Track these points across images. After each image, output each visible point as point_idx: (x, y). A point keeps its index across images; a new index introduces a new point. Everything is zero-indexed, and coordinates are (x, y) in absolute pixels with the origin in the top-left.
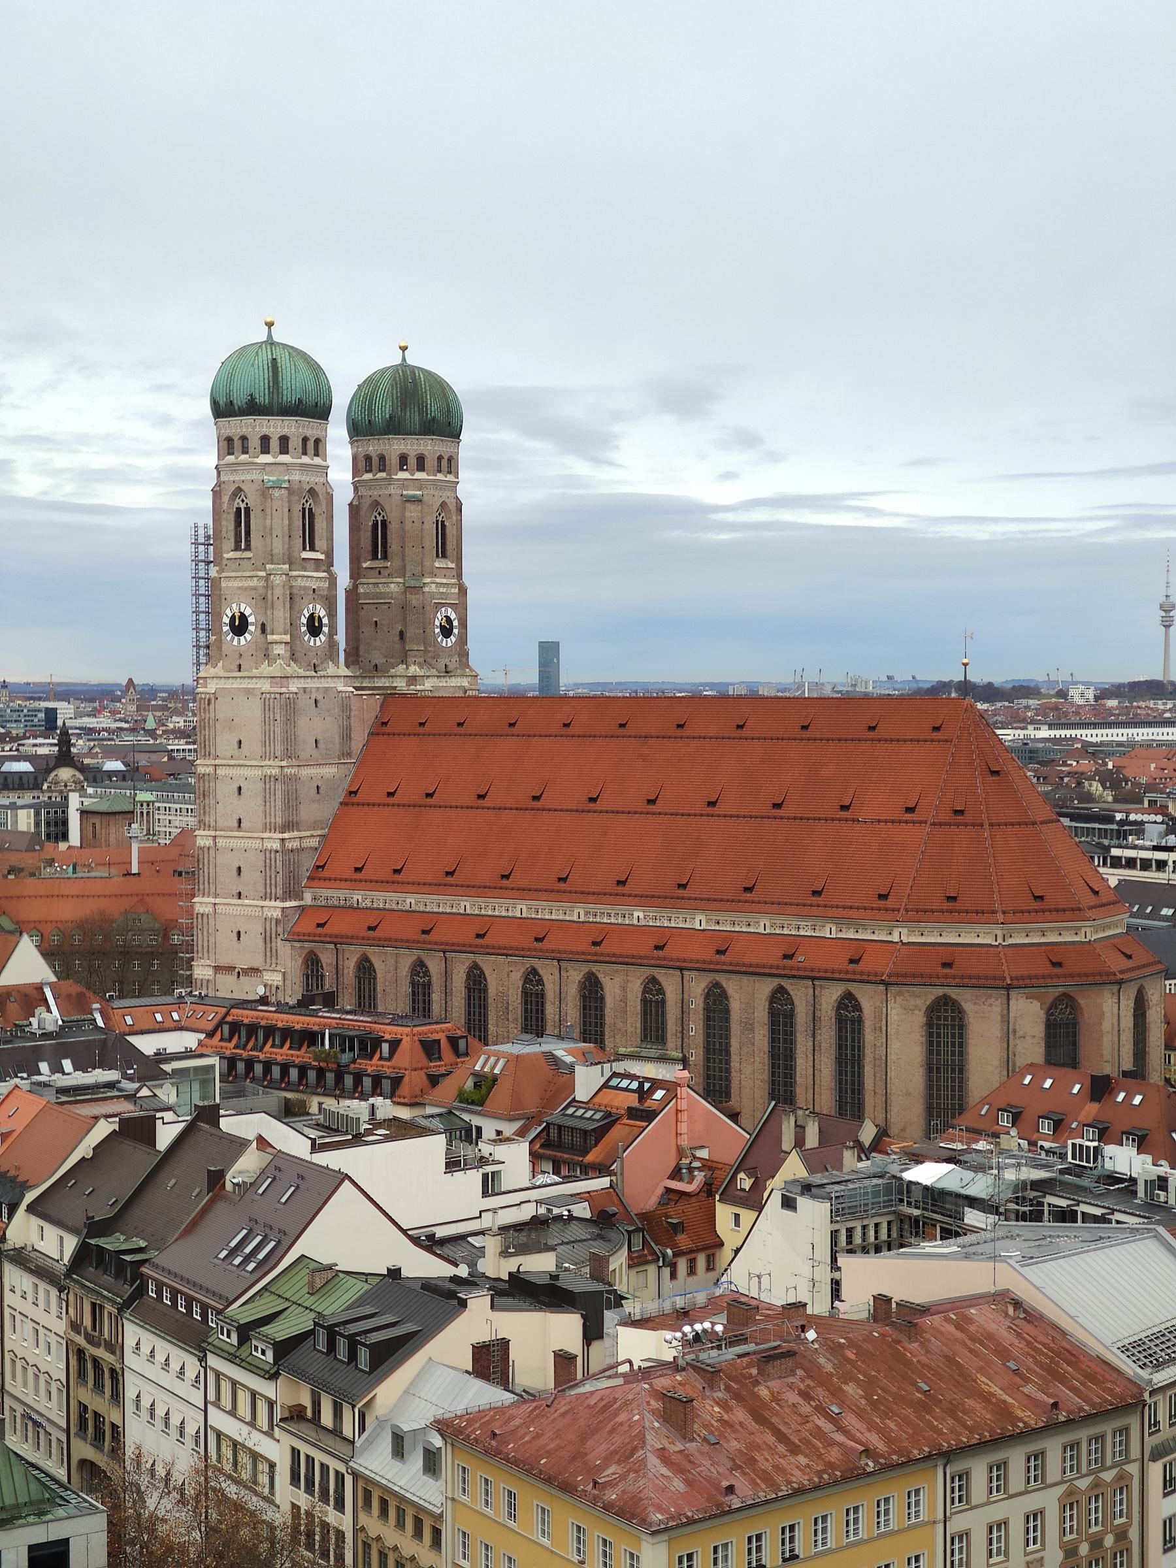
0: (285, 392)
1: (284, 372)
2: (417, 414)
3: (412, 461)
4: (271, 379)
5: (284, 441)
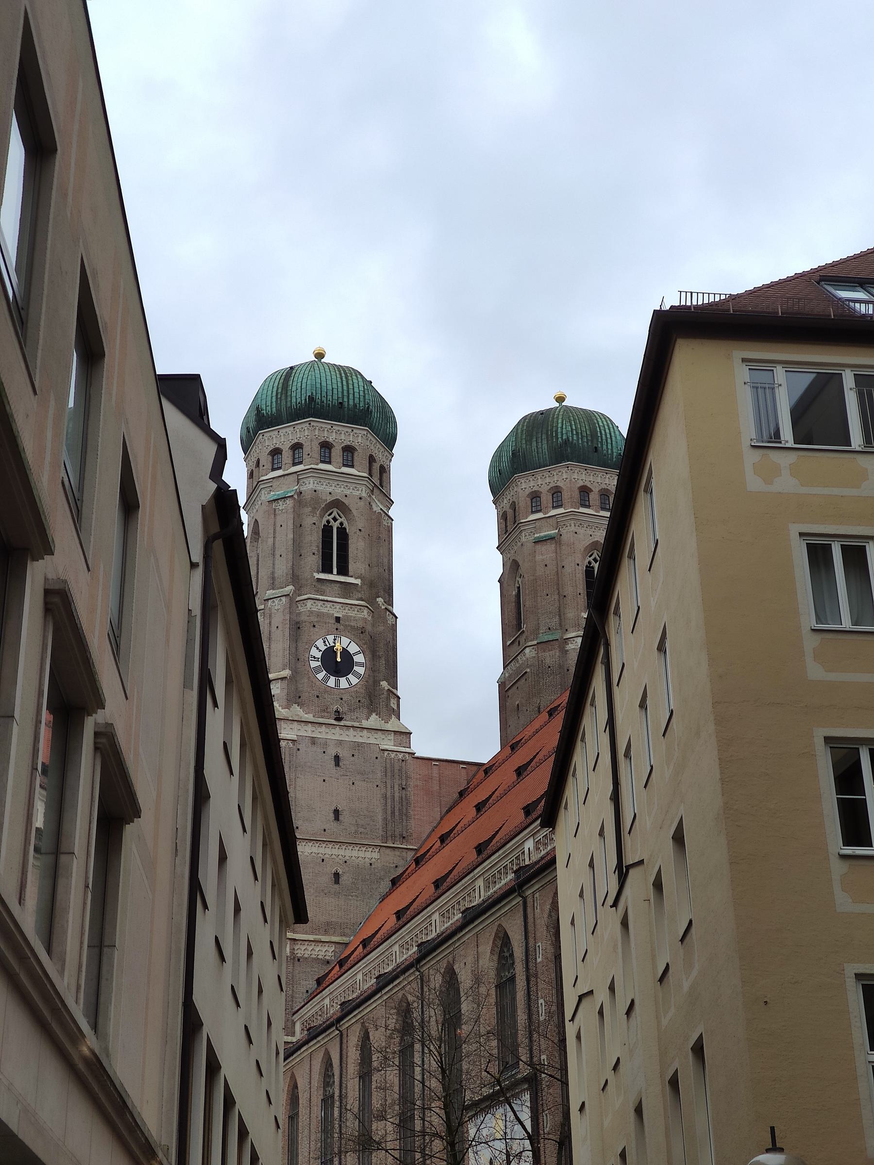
0: (294, 394)
1: (297, 375)
2: (545, 442)
3: (546, 499)
4: (280, 386)
5: (297, 447)
